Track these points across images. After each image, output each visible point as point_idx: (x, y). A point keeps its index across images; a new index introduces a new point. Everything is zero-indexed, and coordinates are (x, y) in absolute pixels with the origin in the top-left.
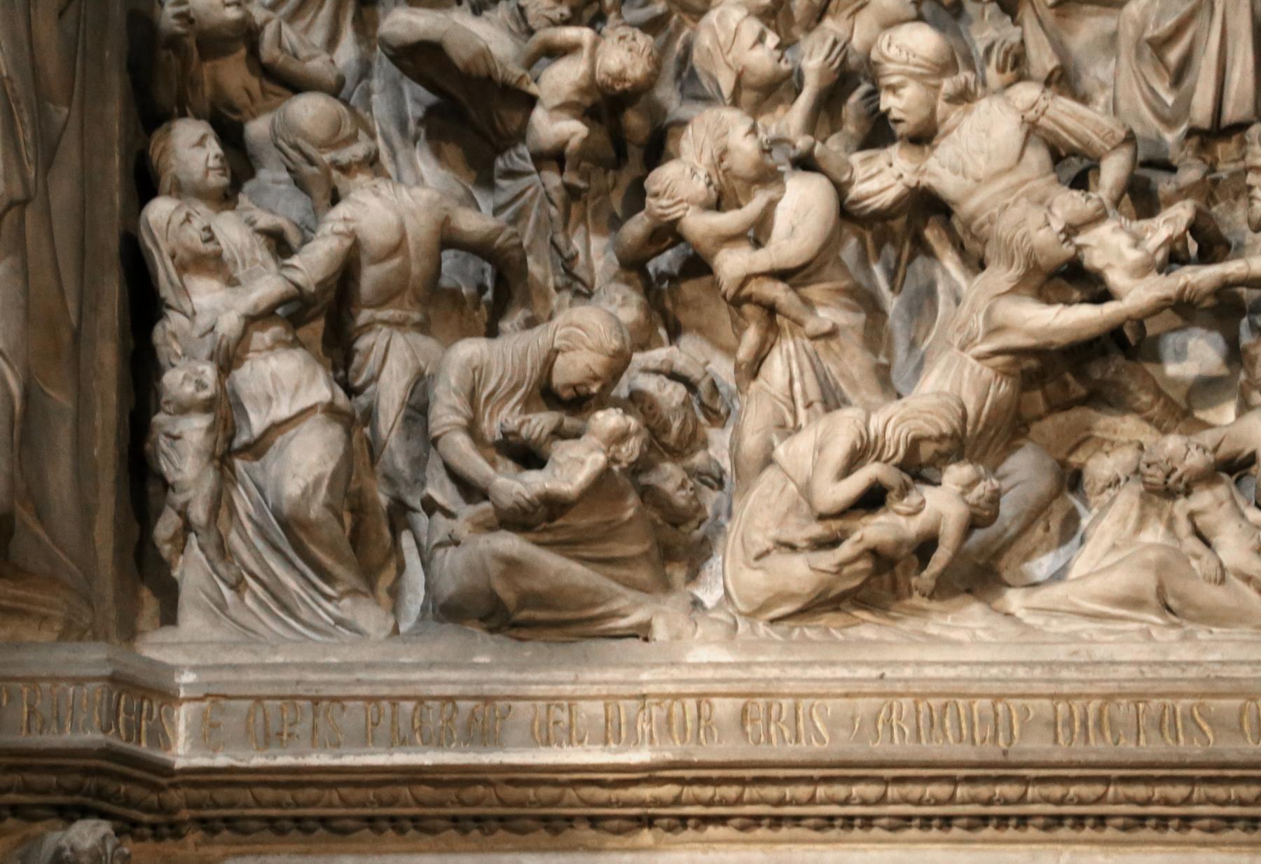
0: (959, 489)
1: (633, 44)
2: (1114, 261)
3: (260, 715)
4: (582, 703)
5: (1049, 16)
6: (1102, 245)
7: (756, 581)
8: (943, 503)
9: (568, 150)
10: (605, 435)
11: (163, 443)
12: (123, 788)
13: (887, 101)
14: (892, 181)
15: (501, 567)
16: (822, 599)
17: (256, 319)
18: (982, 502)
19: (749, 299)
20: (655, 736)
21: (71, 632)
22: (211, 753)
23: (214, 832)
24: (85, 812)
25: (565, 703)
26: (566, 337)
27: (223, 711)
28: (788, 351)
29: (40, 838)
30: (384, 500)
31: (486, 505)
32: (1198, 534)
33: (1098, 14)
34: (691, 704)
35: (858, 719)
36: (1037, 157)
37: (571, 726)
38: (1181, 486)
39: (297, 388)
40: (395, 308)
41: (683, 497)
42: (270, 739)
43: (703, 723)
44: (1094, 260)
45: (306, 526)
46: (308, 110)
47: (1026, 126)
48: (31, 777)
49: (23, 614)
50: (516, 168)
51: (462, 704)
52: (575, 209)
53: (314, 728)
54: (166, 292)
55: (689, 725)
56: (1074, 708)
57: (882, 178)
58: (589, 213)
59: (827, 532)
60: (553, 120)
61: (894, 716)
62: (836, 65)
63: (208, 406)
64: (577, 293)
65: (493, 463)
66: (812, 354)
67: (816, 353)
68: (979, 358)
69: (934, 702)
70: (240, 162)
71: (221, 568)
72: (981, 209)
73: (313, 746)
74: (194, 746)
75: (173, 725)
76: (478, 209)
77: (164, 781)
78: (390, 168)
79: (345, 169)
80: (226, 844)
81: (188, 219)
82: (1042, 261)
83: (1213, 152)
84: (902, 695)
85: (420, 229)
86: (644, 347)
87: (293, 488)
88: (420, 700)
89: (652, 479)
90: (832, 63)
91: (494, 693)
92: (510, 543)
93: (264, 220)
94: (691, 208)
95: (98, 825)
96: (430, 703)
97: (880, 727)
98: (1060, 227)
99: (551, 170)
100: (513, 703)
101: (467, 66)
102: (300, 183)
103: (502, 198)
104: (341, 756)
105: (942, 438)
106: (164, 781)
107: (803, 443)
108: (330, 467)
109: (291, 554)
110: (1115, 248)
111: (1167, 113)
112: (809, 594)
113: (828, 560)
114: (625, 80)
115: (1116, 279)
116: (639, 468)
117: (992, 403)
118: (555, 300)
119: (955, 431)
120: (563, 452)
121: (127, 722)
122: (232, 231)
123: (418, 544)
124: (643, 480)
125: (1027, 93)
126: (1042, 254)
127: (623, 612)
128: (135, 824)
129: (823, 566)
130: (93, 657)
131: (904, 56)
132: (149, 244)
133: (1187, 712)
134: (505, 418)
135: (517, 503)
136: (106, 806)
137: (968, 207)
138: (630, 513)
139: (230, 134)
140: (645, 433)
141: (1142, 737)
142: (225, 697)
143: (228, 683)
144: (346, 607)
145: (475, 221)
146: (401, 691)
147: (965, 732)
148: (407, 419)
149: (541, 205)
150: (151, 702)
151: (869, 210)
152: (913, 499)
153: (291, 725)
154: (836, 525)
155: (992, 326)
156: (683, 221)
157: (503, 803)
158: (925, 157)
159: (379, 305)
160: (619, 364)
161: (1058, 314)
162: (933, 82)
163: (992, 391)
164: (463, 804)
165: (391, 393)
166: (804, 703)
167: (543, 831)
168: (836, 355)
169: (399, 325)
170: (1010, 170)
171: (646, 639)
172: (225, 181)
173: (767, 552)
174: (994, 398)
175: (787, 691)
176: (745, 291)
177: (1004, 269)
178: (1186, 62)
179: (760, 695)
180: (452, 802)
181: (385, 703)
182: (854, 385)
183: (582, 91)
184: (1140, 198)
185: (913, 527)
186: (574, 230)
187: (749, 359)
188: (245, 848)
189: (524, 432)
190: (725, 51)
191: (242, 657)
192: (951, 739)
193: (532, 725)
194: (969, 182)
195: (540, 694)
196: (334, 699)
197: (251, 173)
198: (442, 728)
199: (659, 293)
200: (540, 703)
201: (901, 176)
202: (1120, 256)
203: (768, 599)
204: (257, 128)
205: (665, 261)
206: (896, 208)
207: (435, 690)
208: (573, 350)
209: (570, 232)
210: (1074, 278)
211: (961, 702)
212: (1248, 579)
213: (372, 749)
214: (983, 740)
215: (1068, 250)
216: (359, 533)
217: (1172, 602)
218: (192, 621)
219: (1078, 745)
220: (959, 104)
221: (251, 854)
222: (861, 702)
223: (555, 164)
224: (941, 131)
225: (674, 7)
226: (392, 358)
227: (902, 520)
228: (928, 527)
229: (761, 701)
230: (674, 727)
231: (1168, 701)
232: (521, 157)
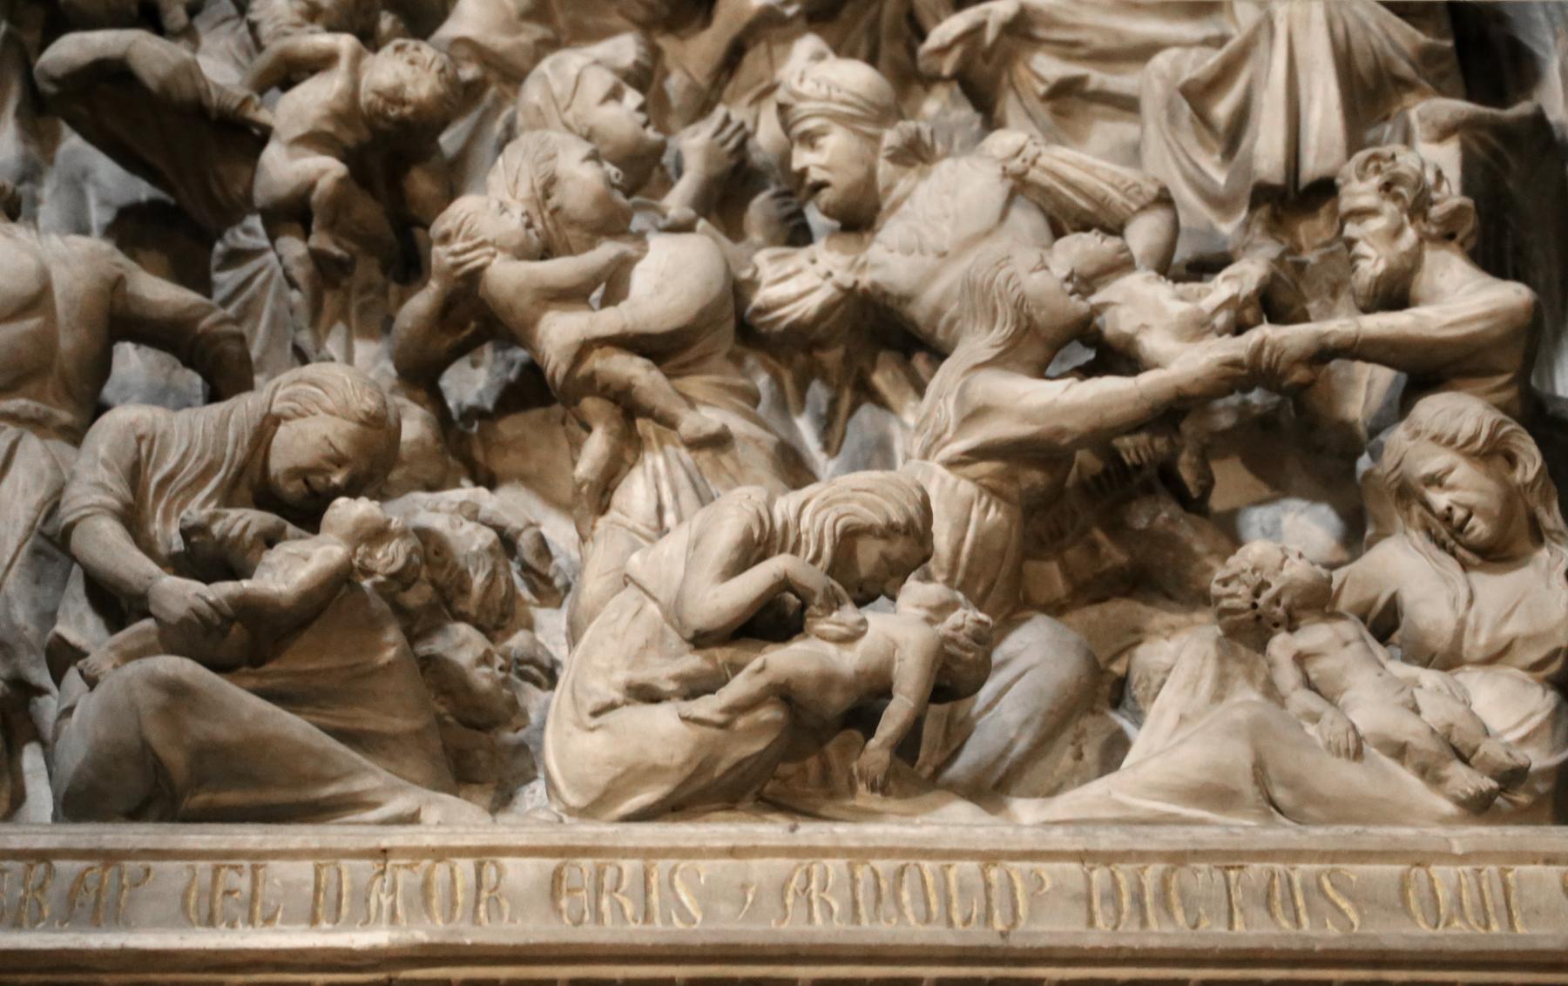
0: (923, 613)
1: (416, 54)
2: (1150, 320)
4: (273, 864)
5: (1043, 111)
6: (1131, 299)
9: (315, 197)
10: (348, 527)
14: (818, 281)
15: (159, 698)
16: (702, 782)
18: (962, 637)
19: (590, 385)
20: (400, 912)
25: (246, 864)
26: (289, 398)
28: (654, 467)
32: (1309, 684)
33: (1113, 119)
34: (465, 866)
35: (753, 889)
37: (253, 897)
38: (1280, 611)
40: (29, 397)
41: (486, 675)
43: (484, 894)
47: (1009, 182)
50: (240, 245)
51: (61, 865)
52: (330, 301)
55: (460, 898)
56: (1120, 876)
58: (353, 311)
59: (708, 666)
60: (292, 157)
61: (814, 885)
62: (732, 144)
66: (692, 469)
67: (699, 469)
68: (951, 464)
69: (881, 865)
82: (1041, 317)
83: (1293, 235)
84: (825, 853)
90: (725, 142)
91: (121, 846)
94: (500, 255)
97: (790, 900)
98: (1065, 273)
99: (291, 233)
100: (152, 864)
101: (164, 85)
107: (674, 545)
112: (681, 768)
113: (707, 707)
114: (403, 103)
115: (1153, 343)
117: (976, 537)
119: (910, 522)
126: (1040, 307)
127: (370, 798)
131: (824, 90)
133: (1313, 883)
135: (193, 609)
138: (390, 654)
141: (1237, 917)
147: (935, 908)
148: (36, 552)
149: (279, 296)
151: (784, 323)
154: (722, 655)
155: (968, 410)
156: (489, 271)
158: (863, 246)
161: (1067, 388)
162: (869, 129)
163: (974, 515)
166: (661, 866)
168: (730, 475)
170: (988, 233)
173: (612, 706)
174: (978, 528)
175: (630, 844)
176: (584, 370)
177: (984, 329)
178: (1242, 117)
179: (586, 852)
185: (849, 661)
186: (328, 331)
187: (593, 477)
189: (217, 528)
190: (562, 105)
192: (911, 919)
193: (185, 896)
194: (930, 260)
195: (201, 847)
198: (23, 901)
199: (464, 437)
200: (201, 865)
201: (829, 274)
202: (1160, 310)
203: (614, 780)
206: (823, 326)
208: (302, 416)
209: (321, 331)
211: (927, 865)
214: (967, 921)
215: (1080, 306)
220: (910, 165)
222: (757, 865)
223: (298, 227)
224: (886, 205)
225: (492, 76)
227: (831, 649)
228: (874, 661)
229: (587, 863)
230: (435, 903)
231: (1279, 867)
232: (249, 231)
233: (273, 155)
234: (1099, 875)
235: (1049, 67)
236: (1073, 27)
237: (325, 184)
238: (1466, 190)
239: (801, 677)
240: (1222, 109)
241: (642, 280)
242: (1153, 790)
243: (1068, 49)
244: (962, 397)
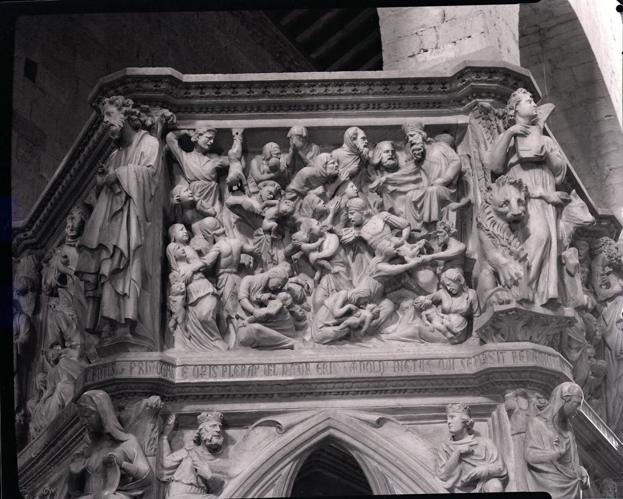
3: (196, 369)
7: (319, 334)
8: (366, 313)
11: (172, 303)
13: (350, 216)
17: (195, 273)
21: (150, 350)
24: (152, 394)
30: (226, 316)
31: (252, 316)
36: (388, 229)
39: (205, 288)
44: (402, 254)
46: (208, 221)
52: (274, 244)
54: (173, 266)
57: (349, 234)
63: (182, 294)
64: (274, 264)
65: (254, 306)
68: (374, 278)
69: (364, 362)
70: (191, 234)
71: (185, 333)
72: (374, 242)
76: (249, 243)
78: (227, 234)
79: (218, 235)
81: (179, 248)
85: (235, 250)
86: (290, 277)
87: (204, 313)
88: (236, 365)
89: (292, 309)
92: (257, 326)
93: (197, 248)
102: (206, 239)
103: (255, 241)
105: (366, 297)
108: (213, 308)
109: (203, 330)
110: (407, 250)
111: (418, 218)
113: (337, 328)
115: (406, 258)
116: (289, 307)
118: (269, 265)
120: (271, 303)
122: (189, 251)
123: (234, 327)
124: (291, 310)
125: (385, 214)
128: (164, 397)
129: (336, 330)
130: (156, 355)
132: (169, 253)
134: (258, 295)
136: (158, 392)
137: (370, 242)
139: (188, 227)
140: (292, 298)
145: (249, 247)
152: (358, 313)
159: (225, 268)
160: (285, 281)
165: (227, 290)
169: (230, 273)
171: (292, 349)
172: (187, 238)
178: (422, 206)
179: (322, 362)
181: (227, 366)
182: (343, 285)
183: (276, 215)
184: (411, 239)
191: (191, 355)
196: (216, 365)
197: (193, 236)
204: (195, 226)
205: (296, 256)
210: (395, 258)
211: (371, 362)
212: (440, 331)
215: (395, 251)
216: (220, 324)
217: (422, 337)
218: (178, 346)
219: (400, 372)
226: (228, 279)
233: (265, 221)
234: (396, 363)
235: (391, 188)
236: (395, 180)
237: (274, 227)
238: (456, 228)
239: (351, 324)
240: (419, 206)
241: (325, 245)
242: (403, 336)
243: (394, 184)
244: (376, 267)
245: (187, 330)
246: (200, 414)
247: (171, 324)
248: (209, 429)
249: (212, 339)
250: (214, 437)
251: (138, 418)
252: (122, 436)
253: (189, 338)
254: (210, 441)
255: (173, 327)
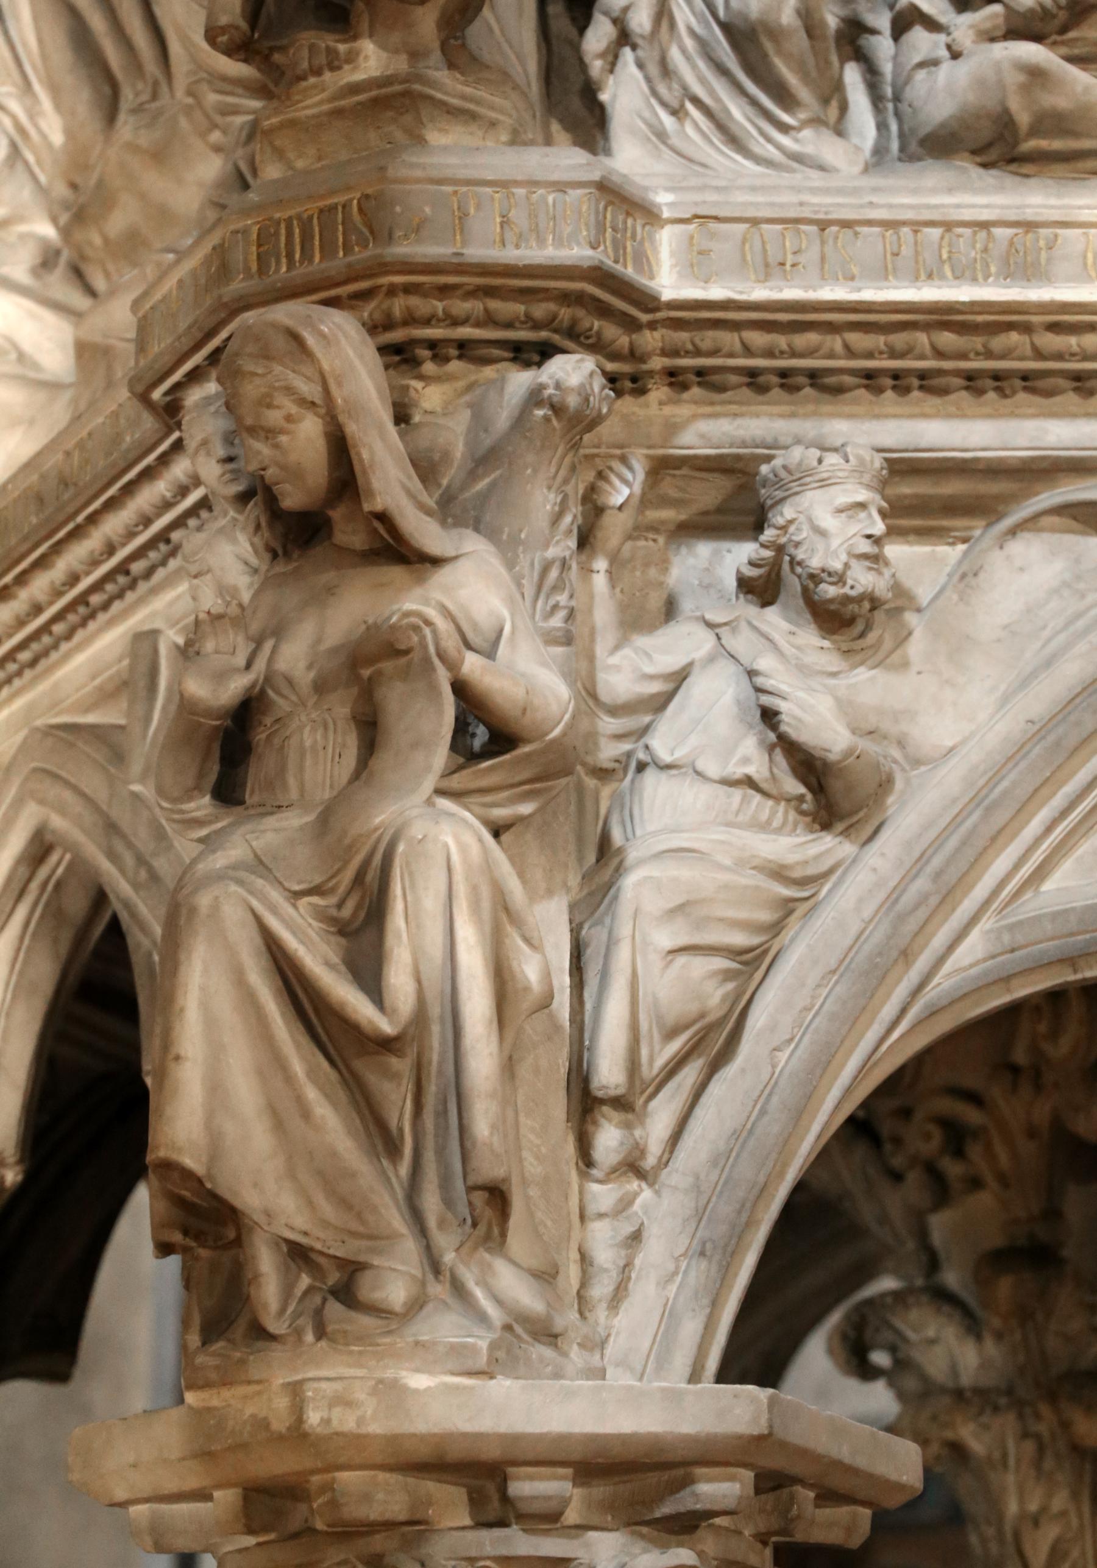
12: (596, 324)
15: (1022, 78)
22: (702, 284)
23: (685, 387)
27: (712, 235)
29: (500, 384)
42: (770, 269)
45: (776, 34)
48: (495, 305)
49: (473, 116)
51: (998, 231)
53: (823, 259)
73: (823, 278)
74: (681, 275)
75: (656, 251)
77: (644, 318)
80: (696, 403)
88: (948, 226)
95: (582, 360)
96: (960, 230)
100: (1059, 231)
104: (859, 290)
106: (644, 318)
121: (615, 241)
142: (716, 218)
143: (716, 204)
144: (811, 141)
146: (926, 216)
150: (635, 220)
153: (795, 253)
157: (1039, 354)
164: (989, 354)
167: (1071, 394)
180: (978, 354)
181: (905, 230)
188: (718, 409)
193: (1085, 257)
196: (846, 224)
198: (975, 260)
207: (967, 215)
213: (894, 282)
221: (725, 415)
245: (666, 70)
246: (769, 459)
247: (598, 36)
248: (828, 521)
249: (785, 118)
250: (854, 563)
251: (484, 460)
252: (425, 532)
253: (677, 112)
254: (840, 579)
255: (602, 55)
